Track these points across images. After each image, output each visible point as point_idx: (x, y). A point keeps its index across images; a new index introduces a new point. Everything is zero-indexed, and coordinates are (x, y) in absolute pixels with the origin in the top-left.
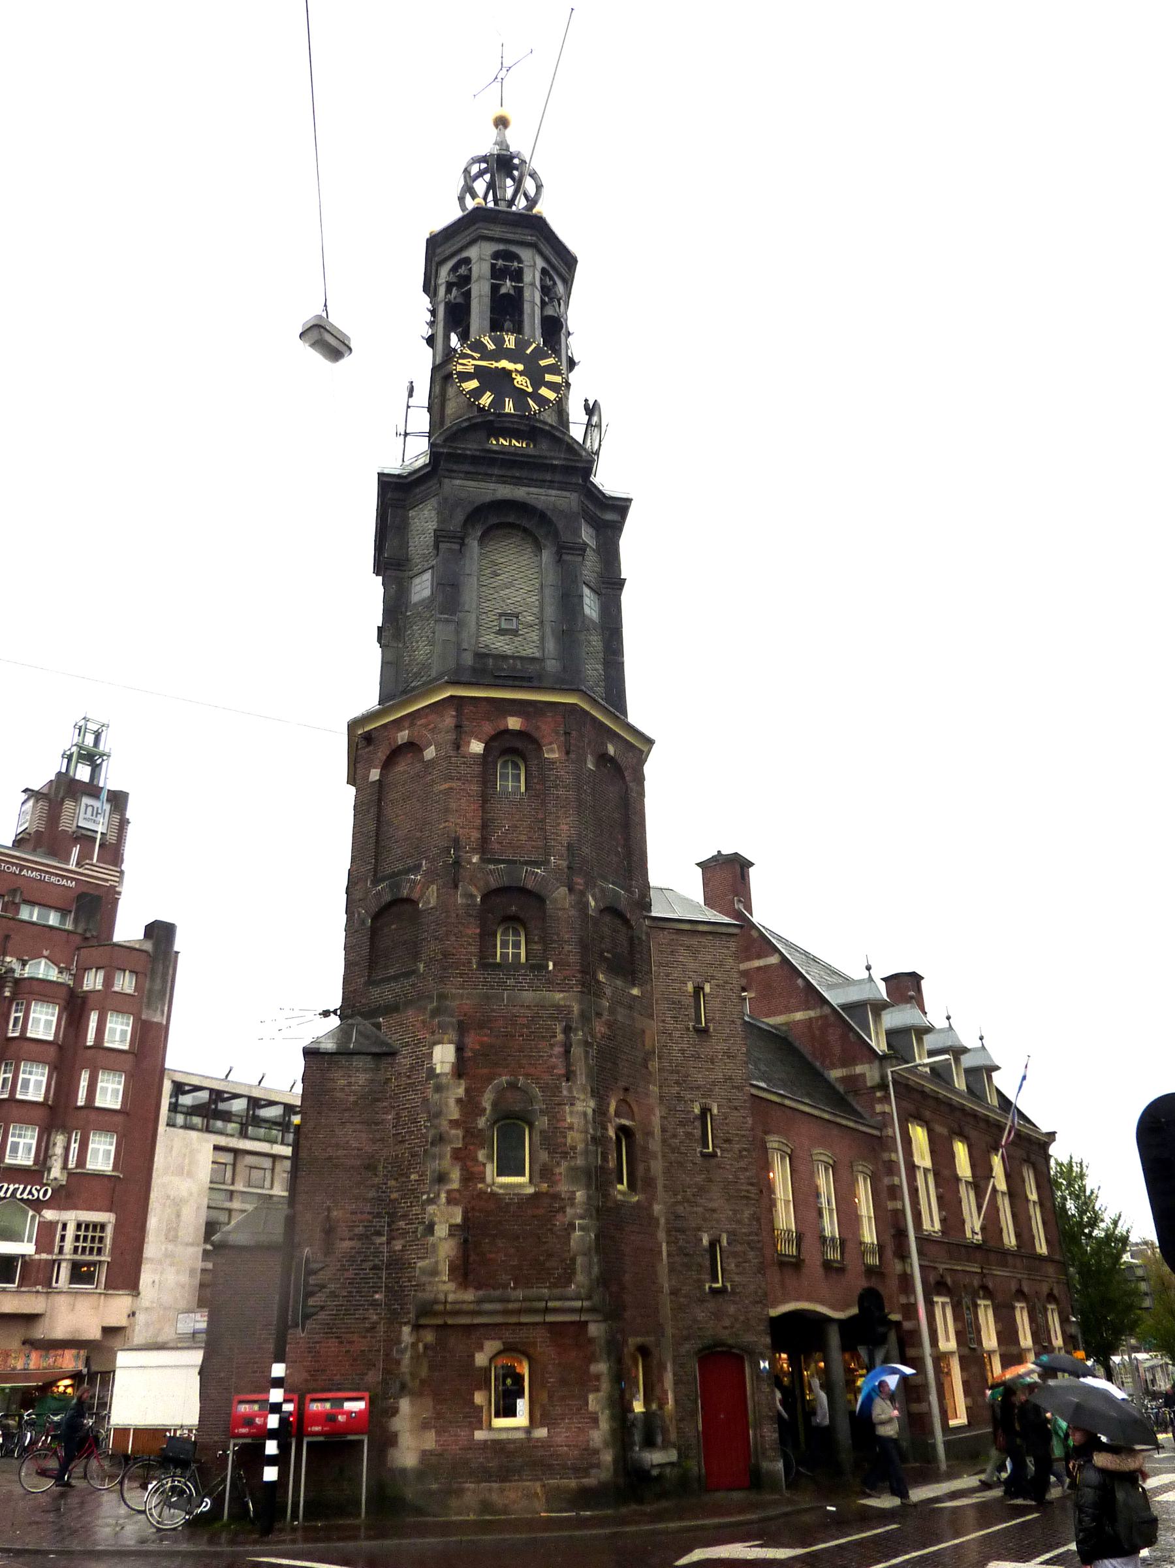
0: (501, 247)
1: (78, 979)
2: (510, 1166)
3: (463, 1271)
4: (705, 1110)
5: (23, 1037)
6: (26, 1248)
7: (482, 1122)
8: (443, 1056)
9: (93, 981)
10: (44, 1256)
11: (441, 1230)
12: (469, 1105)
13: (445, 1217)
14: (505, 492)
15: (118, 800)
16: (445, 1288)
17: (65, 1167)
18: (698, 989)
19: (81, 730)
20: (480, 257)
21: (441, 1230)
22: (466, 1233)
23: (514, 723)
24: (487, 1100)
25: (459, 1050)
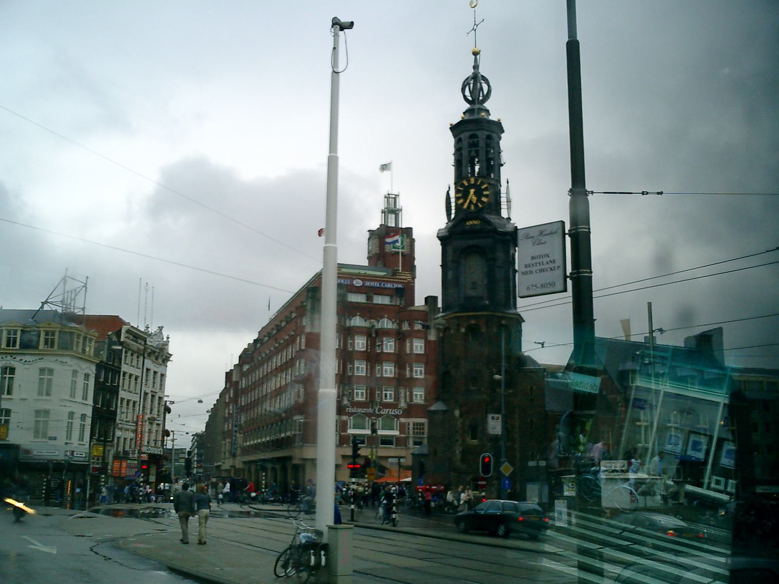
0: (472, 133)
1: (400, 325)
2: (474, 438)
3: (463, 461)
4: (532, 421)
5: (382, 353)
6: (396, 433)
7: (466, 428)
8: (457, 413)
9: (406, 327)
10: (403, 435)
11: (457, 452)
12: (463, 423)
13: (458, 450)
14: (471, 242)
15: (408, 231)
16: (458, 464)
17: (406, 402)
18: (531, 388)
19: (387, 197)
20: (464, 136)
21: (457, 452)
22: (464, 453)
23: (473, 322)
24: (467, 423)
25: (461, 411)
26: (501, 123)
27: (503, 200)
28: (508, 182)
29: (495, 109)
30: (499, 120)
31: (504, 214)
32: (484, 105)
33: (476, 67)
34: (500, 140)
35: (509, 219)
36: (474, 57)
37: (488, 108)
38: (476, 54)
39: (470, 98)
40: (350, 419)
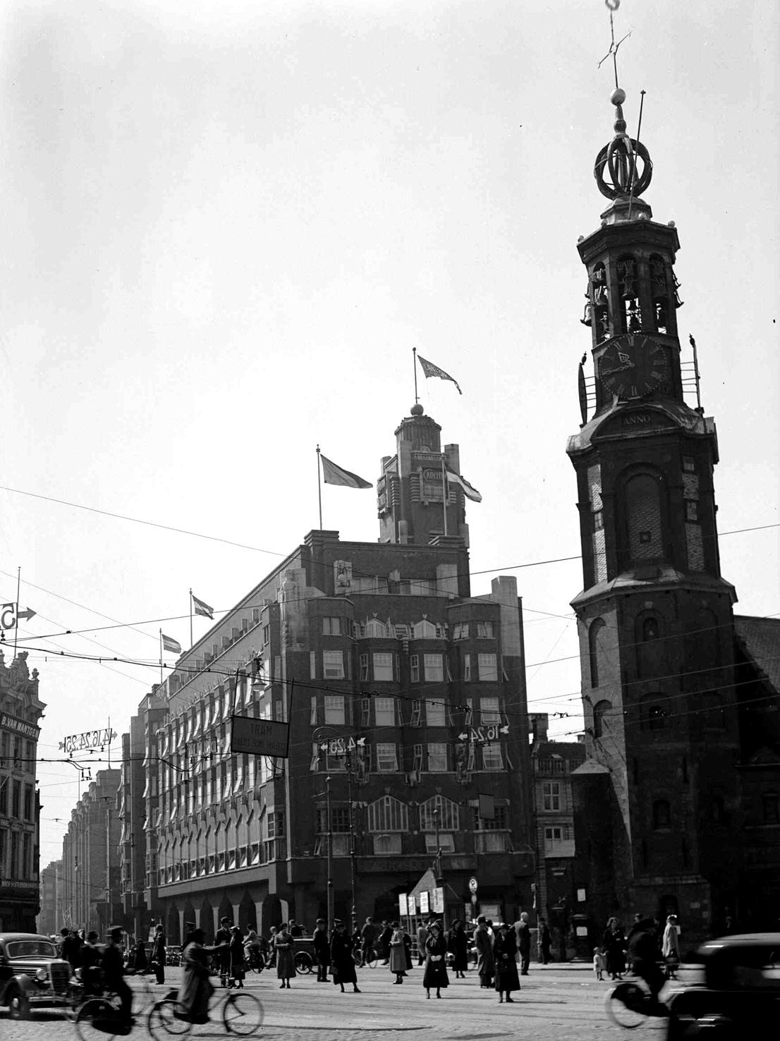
23: (649, 604)
26: (675, 230)
27: (687, 374)
28: (692, 342)
29: (662, 203)
30: (672, 224)
31: (690, 401)
32: (641, 197)
33: (620, 126)
34: (673, 263)
35: (700, 410)
36: (616, 107)
37: (648, 203)
38: (618, 100)
39: (612, 187)
40: (372, 807)
